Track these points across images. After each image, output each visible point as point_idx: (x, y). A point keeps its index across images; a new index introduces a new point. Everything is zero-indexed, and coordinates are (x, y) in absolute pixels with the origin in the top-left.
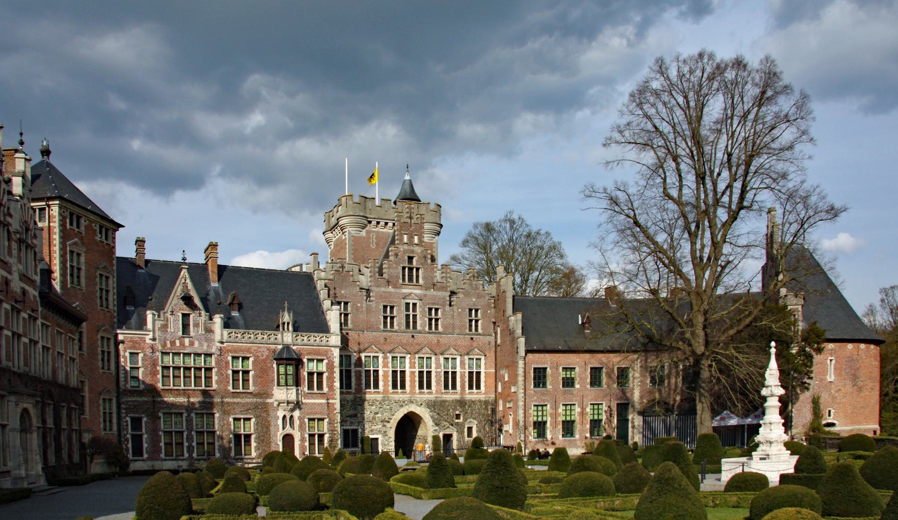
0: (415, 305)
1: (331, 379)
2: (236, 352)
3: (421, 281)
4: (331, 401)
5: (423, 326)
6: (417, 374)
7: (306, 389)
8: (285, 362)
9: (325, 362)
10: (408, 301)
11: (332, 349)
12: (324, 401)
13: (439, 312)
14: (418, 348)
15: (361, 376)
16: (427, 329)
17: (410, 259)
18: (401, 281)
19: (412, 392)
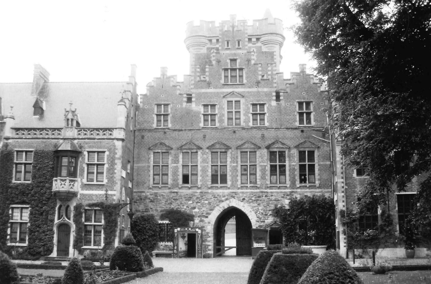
0: (238, 102)
1: (111, 170)
2: (20, 147)
3: (245, 81)
4: (110, 192)
5: (247, 121)
6: (239, 168)
7: (85, 181)
8: (69, 154)
9: (107, 153)
10: (230, 99)
11: (115, 141)
12: (103, 192)
13: (266, 107)
14: (240, 143)
15: (177, 171)
16: (251, 124)
17: (233, 60)
18: (222, 81)
19: (233, 186)
